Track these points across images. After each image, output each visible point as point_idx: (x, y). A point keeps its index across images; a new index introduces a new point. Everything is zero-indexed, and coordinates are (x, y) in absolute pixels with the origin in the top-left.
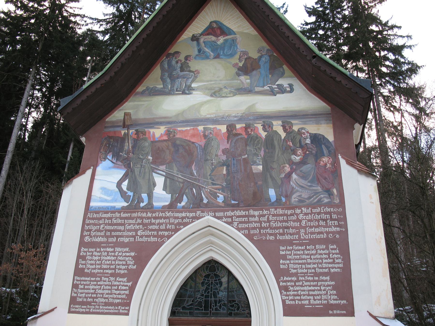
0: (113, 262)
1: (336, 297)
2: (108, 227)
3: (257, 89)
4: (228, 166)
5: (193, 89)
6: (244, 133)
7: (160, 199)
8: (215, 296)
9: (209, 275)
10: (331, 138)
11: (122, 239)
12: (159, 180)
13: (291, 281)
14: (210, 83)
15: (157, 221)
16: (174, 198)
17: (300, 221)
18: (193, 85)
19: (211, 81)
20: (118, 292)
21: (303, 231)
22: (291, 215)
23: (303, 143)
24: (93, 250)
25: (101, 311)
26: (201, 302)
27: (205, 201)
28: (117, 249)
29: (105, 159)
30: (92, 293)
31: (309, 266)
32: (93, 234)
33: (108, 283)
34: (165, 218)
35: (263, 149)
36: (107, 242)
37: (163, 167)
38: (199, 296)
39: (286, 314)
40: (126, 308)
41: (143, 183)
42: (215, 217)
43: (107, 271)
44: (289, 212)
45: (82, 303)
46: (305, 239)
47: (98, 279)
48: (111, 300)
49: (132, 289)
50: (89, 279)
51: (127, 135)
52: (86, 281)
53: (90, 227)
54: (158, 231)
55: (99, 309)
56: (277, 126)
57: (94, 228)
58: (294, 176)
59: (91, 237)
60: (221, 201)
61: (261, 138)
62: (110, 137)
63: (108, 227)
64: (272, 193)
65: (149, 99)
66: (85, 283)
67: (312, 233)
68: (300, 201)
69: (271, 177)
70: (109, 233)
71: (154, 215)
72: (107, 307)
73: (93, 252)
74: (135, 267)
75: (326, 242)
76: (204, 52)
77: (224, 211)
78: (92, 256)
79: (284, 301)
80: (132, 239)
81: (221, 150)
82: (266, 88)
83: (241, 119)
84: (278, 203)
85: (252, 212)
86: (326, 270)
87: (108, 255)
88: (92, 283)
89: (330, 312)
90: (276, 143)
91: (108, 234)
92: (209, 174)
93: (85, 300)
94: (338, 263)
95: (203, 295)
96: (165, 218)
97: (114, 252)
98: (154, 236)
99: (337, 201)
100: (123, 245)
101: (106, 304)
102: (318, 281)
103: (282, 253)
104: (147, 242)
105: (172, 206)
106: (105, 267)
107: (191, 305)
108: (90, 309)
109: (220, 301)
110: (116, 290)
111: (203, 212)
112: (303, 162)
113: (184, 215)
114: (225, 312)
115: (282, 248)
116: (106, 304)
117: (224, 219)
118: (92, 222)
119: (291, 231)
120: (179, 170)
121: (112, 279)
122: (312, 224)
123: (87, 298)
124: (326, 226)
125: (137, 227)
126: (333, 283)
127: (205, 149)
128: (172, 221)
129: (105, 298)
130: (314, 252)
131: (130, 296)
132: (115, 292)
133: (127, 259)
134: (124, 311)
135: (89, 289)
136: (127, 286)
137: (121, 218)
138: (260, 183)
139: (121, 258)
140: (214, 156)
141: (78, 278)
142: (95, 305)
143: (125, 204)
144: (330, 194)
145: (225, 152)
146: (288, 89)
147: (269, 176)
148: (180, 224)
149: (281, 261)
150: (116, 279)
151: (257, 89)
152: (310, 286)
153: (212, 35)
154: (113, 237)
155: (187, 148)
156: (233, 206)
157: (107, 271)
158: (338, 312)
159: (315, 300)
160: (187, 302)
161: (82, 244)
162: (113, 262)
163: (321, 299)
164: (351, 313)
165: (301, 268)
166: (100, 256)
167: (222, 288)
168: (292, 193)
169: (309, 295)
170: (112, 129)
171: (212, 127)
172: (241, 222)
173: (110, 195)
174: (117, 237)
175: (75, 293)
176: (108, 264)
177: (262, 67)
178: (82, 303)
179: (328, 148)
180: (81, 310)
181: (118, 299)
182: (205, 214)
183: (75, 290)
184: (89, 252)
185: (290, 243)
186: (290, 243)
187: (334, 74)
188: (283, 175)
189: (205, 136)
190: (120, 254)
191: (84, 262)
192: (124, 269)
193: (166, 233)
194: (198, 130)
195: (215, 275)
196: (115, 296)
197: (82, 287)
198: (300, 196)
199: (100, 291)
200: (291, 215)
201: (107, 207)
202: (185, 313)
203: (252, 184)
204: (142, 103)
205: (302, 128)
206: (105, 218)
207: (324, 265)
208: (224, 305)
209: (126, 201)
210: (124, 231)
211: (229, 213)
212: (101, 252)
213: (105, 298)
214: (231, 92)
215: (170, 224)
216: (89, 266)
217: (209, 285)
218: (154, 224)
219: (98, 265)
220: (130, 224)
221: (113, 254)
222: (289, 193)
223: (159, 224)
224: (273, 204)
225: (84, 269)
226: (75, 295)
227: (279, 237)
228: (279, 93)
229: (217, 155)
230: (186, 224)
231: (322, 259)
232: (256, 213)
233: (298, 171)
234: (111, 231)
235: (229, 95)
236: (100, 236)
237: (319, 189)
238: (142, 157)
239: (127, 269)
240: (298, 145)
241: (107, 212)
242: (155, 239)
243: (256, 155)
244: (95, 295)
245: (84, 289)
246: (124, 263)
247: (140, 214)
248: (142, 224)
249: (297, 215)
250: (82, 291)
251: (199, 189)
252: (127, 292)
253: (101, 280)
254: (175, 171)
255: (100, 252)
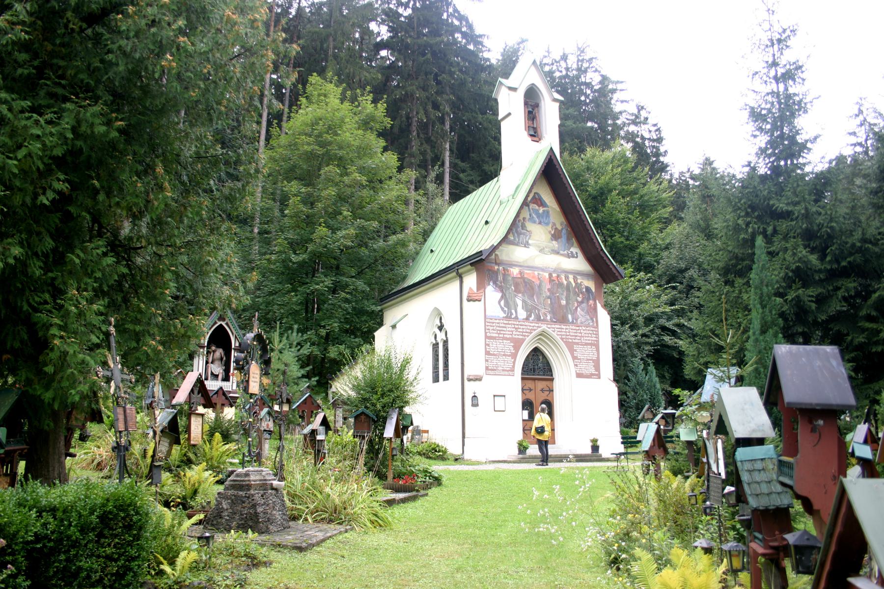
2: (498, 328)
3: (562, 252)
10: (594, 290)
11: (505, 336)
18: (530, 242)
27: (542, 318)
28: (505, 341)
29: (489, 284)
37: (520, 295)
41: (511, 303)
49: (514, 363)
51: (498, 269)
53: (489, 327)
54: (523, 332)
56: (571, 277)
57: (491, 328)
58: (579, 309)
63: (498, 328)
64: (570, 317)
65: (507, 246)
68: (582, 323)
75: (591, 344)
76: (533, 217)
82: (565, 252)
83: (555, 271)
85: (563, 327)
100: (507, 339)
101: (503, 370)
105: (527, 319)
112: (582, 302)
127: (540, 286)
131: (514, 366)
144: (593, 321)
145: (548, 289)
151: (562, 252)
161: (486, 337)
164: (599, 378)
185: (577, 344)
186: (577, 344)
187: (609, 263)
189: (539, 279)
211: (553, 326)
230: (535, 330)
232: (564, 327)
237: (588, 317)
243: (562, 294)
251: (539, 310)
254: (526, 299)
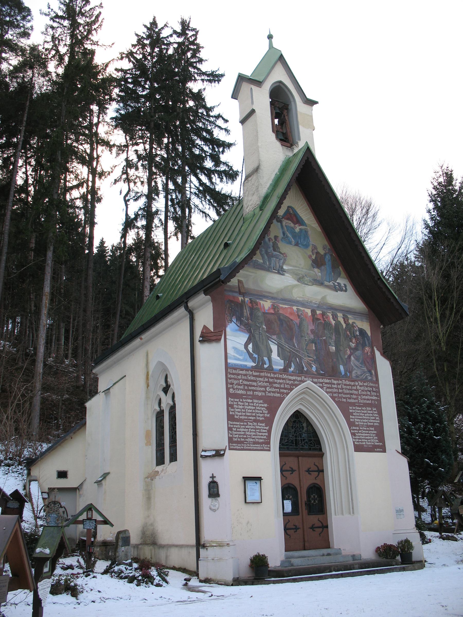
0: (254, 411)
1: (377, 441)
2: (246, 383)
3: (326, 283)
4: (315, 344)
5: (284, 271)
6: (321, 318)
7: (277, 364)
8: (301, 437)
9: (296, 421)
10: (369, 333)
11: (256, 393)
12: (274, 348)
13: (356, 430)
14: (295, 268)
15: (278, 381)
16: (286, 364)
17: (358, 390)
18: (285, 267)
19: (296, 267)
20: (260, 434)
21: (360, 397)
22: (354, 386)
23: (355, 335)
24: (238, 400)
25: (252, 448)
26: (292, 441)
27: (305, 369)
28: (255, 401)
29: (231, 321)
30: (243, 435)
31: (364, 421)
32: (235, 387)
33: (252, 427)
34: (283, 379)
35: (334, 335)
36: (246, 395)
37: (274, 337)
38: (291, 436)
39: (356, 450)
40: (268, 446)
41: (263, 348)
42: (312, 382)
43: (250, 418)
44: (352, 383)
45: (237, 442)
46: (361, 403)
47: (246, 424)
48: (257, 440)
49: (269, 432)
50: (238, 423)
51: (243, 301)
52: (237, 425)
53: (233, 381)
54: (280, 388)
55: (250, 446)
57: (235, 382)
58: (352, 358)
59: (234, 389)
60: (314, 370)
61: (332, 325)
62: (232, 301)
63: (246, 383)
64: (342, 368)
65: (254, 271)
66: (236, 426)
67: (365, 399)
68: (357, 377)
69: (340, 356)
70: (247, 388)
71: (275, 376)
72: (255, 445)
73: (237, 402)
74: (269, 415)
75: (370, 405)
76: (287, 237)
77: (318, 378)
78: (238, 405)
79: (354, 442)
80: (263, 394)
81: (310, 330)
82: (331, 283)
83: (319, 307)
84: (345, 377)
85: (333, 381)
86: (372, 424)
87: (249, 405)
88: (242, 427)
89: (376, 450)
90: (341, 331)
91: (246, 388)
92: (305, 348)
93: (239, 439)
94: (377, 420)
95: (293, 435)
96: (283, 379)
97: (253, 403)
98: (278, 393)
99: (375, 379)
100: (259, 398)
101: (255, 443)
102: (369, 430)
103: (351, 411)
104: (274, 396)
105: (285, 370)
106: (248, 414)
107: (287, 442)
108: (244, 446)
109: (304, 440)
110: (259, 432)
111: (305, 377)
112: (356, 349)
113: (294, 378)
114: (307, 447)
115: (350, 408)
116: (255, 443)
117: (318, 384)
118: (232, 376)
119: (354, 397)
120: (285, 341)
121: (255, 424)
122: (364, 393)
123: (240, 438)
124: (371, 396)
125: (266, 384)
126: (376, 432)
127: (300, 326)
128: (288, 382)
129: (253, 438)
130: (366, 412)
131: (269, 437)
132: (259, 434)
133: (263, 409)
134: (267, 448)
135: (241, 431)
136: (265, 429)
137: (254, 376)
138: (335, 360)
139: (258, 408)
140: (306, 334)
141: (231, 423)
142: (246, 444)
143: (254, 365)
144: (371, 374)
145: (312, 331)
146: (344, 289)
147: (339, 356)
148: (292, 385)
149: (351, 417)
150: (257, 424)
151: (326, 283)
152: (365, 433)
153: (290, 220)
154: (250, 390)
155: (288, 323)
156: (322, 375)
157: (250, 418)
158: (379, 450)
159: (368, 442)
160: (284, 441)
161: (229, 395)
162: (254, 411)
163: (371, 442)
164: (384, 451)
165: (360, 422)
166: (243, 405)
167: (304, 431)
168: (352, 370)
169: (365, 439)
170: (231, 294)
171: (302, 309)
172: (328, 388)
173: (241, 355)
174: (254, 391)
175: (231, 434)
176: (250, 413)
177: (327, 264)
178: (237, 442)
179: (368, 340)
180: (238, 447)
181: (262, 439)
182: (307, 379)
183: (231, 432)
184: (235, 402)
185: (353, 404)
186: (353, 404)
187: (390, 296)
188: (346, 357)
189: (299, 316)
190: (257, 405)
191: (232, 410)
192: (262, 417)
193: (285, 391)
194: (293, 310)
195: (299, 421)
196: (259, 437)
197: (235, 429)
198: (356, 373)
199: (248, 433)
200: (354, 386)
201: (237, 365)
202: (284, 448)
203: (331, 360)
204: (250, 274)
205: (354, 323)
206: (242, 374)
207: (371, 421)
208: (306, 442)
209: (254, 362)
210: (257, 387)
211: (321, 380)
212: (244, 402)
213: (253, 438)
214: (310, 281)
215: (288, 384)
216: (237, 413)
217: (296, 429)
218: (276, 383)
219: (244, 412)
220: (260, 381)
221: (252, 404)
222: (351, 370)
223: (280, 383)
224: (343, 376)
225: (233, 415)
226: (231, 436)
227: (349, 400)
228: (339, 290)
229: (308, 334)
230: (297, 385)
231: (370, 416)
232: (335, 382)
233: (354, 355)
234: (248, 386)
235: (309, 284)
236: (241, 389)
237: (365, 369)
238: (258, 325)
239: (264, 417)
240: (353, 336)
241: (242, 370)
242: (278, 395)
243: (331, 338)
244: (245, 436)
245: (237, 431)
246: (261, 412)
247: (266, 374)
248: (268, 382)
249: (356, 386)
250: (236, 433)
251: (301, 359)
252: (267, 434)
253: (247, 425)
254: (283, 342)
255: (243, 402)
